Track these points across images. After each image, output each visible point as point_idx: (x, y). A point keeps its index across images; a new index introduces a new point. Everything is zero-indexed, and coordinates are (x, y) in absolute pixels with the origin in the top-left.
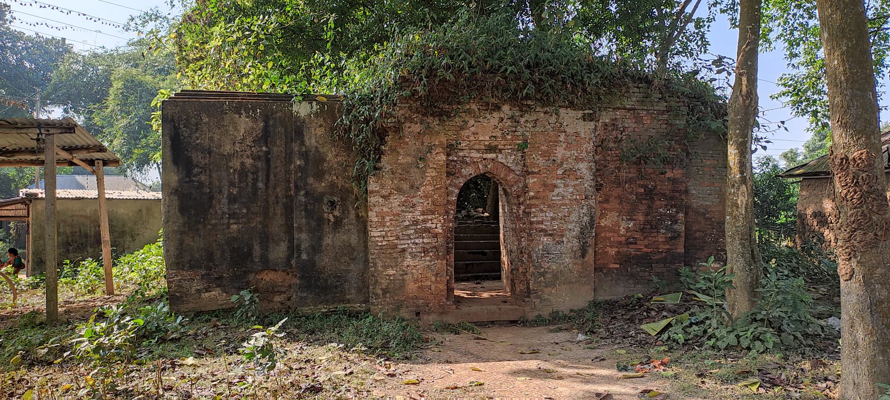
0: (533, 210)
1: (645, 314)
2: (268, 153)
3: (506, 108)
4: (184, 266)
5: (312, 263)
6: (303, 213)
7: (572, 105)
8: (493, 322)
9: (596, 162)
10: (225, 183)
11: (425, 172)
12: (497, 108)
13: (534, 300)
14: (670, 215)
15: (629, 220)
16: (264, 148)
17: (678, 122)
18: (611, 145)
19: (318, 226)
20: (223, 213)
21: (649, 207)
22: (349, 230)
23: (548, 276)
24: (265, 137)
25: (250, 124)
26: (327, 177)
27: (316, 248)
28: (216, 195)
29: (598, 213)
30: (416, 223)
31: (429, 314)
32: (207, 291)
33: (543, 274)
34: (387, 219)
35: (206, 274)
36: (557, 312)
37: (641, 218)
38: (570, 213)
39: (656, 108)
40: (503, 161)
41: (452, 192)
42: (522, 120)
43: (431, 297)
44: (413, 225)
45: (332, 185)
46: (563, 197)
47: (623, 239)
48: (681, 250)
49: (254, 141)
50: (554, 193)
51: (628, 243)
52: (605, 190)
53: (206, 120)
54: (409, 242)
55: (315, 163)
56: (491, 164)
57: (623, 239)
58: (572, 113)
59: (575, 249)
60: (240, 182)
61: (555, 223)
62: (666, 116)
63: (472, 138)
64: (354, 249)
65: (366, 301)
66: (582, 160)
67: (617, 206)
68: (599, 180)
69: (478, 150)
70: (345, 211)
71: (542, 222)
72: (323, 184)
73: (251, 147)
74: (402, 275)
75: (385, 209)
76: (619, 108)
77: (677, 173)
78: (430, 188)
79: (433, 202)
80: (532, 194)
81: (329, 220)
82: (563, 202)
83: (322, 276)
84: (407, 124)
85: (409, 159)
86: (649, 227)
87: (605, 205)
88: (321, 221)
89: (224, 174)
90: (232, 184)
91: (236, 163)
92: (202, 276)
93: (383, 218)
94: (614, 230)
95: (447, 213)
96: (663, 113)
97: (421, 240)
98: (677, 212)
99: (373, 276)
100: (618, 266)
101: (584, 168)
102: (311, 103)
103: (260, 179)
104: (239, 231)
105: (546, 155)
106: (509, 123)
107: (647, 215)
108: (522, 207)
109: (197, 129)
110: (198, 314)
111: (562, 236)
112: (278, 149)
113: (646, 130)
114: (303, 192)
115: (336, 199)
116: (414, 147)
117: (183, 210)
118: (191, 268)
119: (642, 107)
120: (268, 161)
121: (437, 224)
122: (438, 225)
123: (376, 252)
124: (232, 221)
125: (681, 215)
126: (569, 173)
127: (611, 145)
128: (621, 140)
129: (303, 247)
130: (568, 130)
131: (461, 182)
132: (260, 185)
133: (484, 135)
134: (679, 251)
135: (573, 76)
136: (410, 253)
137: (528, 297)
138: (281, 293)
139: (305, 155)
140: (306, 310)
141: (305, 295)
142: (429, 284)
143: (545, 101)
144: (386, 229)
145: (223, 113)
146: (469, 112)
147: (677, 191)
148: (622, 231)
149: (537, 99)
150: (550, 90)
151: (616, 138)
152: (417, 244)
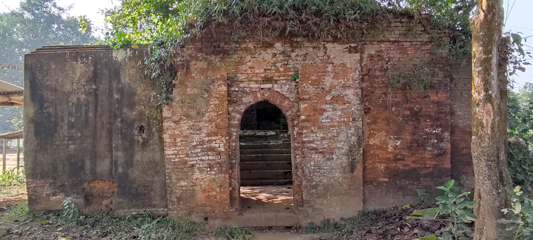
0: (305, 131)
1: (399, 229)
2: (96, 90)
3: (278, 45)
4: (37, 177)
5: (125, 174)
6: (119, 136)
7: (336, 40)
8: (270, 228)
9: (362, 89)
10: (66, 113)
11: (209, 101)
12: (271, 45)
13: (307, 209)
15: (396, 139)
16: (94, 87)
17: (441, 51)
18: (378, 73)
19: (130, 146)
20: (65, 136)
21: (415, 128)
22: (154, 149)
23: (320, 188)
24: (95, 78)
25: (84, 69)
26: (137, 107)
27: (129, 164)
28: (60, 124)
29: (367, 133)
30: (202, 143)
31: (215, 219)
32: (54, 195)
33: (315, 187)
34: (178, 140)
35: (52, 183)
36: (328, 220)
37: (408, 137)
38: (338, 134)
39: (419, 39)
40: (279, 90)
41: (234, 117)
42: (293, 55)
43: (216, 205)
44: (200, 145)
45: (141, 113)
46: (332, 120)
47: (391, 156)
48: (448, 165)
49: (86, 82)
50: (323, 117)
51: (396, 160)
52: (374, 113)
53: (53, 67)
54: (197, 159)
55: (128, 97)
56: (268, 93)
58: (338, 47)
59: (344, 165)
60: (77, 113)
61: (324, 142)
62: (429, 47)
63: (249, 72)
64: (157, 164)
65: (167, 207)
66: (349, 87)
67: (385, 127)
68: (367, 104)
69: (256, 82)
70: (151, 134)
71: (313, 142)
72: (134, 113)
73: (84, 86)
74: (192, 186)
75: (176, 132)
76: (383, 41)
77: (442, 96)
78: (214, 114)
79: (216, 126)
80: (303, 117)
81: (139, 142)
82: (332, 124)
83: (134, 185)
84: (194, 62)
85: (196, 91)
86: (416, 145)
87: (373, 126)
88: (132, 142)
89: (65, 107)
90: (70, 114)
91: (73, 99)
92: (50, 184)
93: (175, 139)
94: (383, 147)
95: (230, 135)
96: (426, 43)
97: (207, 158)
98: (443, 132)
99: (169, 187)
100: (387, 180)
101: (351, 94)
102: (126, 50)
103: (90, 110)
104: (75, 150)
105: (317, 83)
106: (281, 57)
107: (414, 134)
108: (296, 129)
109: (47, 74)
110: (48, 212)
111: (332, 154)
112: (103, 87)
113: (411, 60)
114: (119, 120)
115: (143, 124)
116: (200, 81)
117: (37, 134)
118: (42, 178)
119: (406, 39)
120: (96, 96)
121: (220, 144)
122: (221, 145)
123: (170, 167)
124: (70, 142)
125: (447, 134)
126: (337, 99)
127: (378, 73)
128: (387, 69)
129: (119, 163)
130: (335, 62)
132: (91, 115)
134: (445, 166)
135: (336, 15)
136: (198, 168)
137: (302, 206)
138: (107, 198)
139: (121, 91)
140: (121, 213)
141: (121, 200)
142: (214, 193)
143: (311, 37)
144: (177, 148)
145: (65, 61)
146: (246, 50)
147: (441, 113)
148: (390, 149)
149: (304, 36)
150: (315, 29)
151: (382, 67)
152: (203, 160)
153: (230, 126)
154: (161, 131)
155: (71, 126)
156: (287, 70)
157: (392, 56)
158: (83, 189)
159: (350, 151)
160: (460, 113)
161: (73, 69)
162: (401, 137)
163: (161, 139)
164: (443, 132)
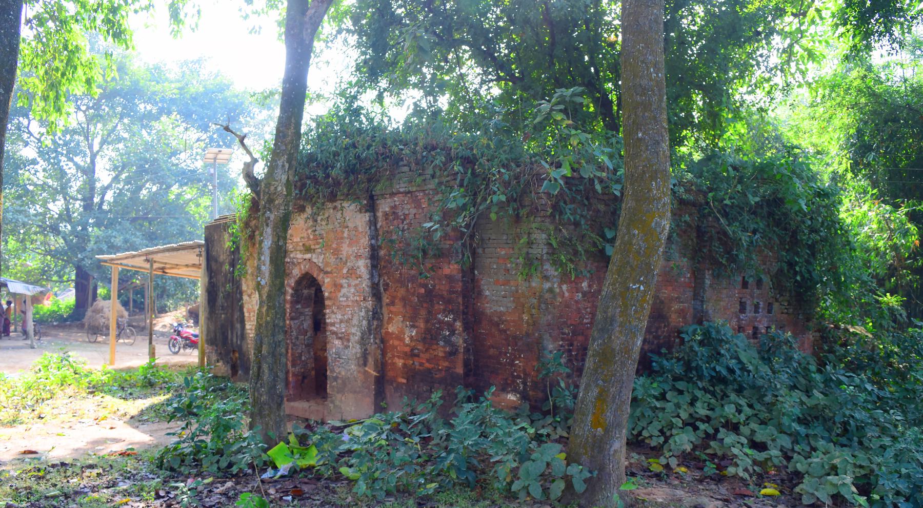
14: (448, 323)
21: (429, 312)
23: (340, 381)
37: (422, 325)
40: (315, 260)
46: (347, 298)
47: (407, 349)
57: (407, 349)
61: (343, 325)
67: (402, 310)
86: (429, 337)
87: (392, 308)
98: (455, 320)
148: (407, 341)
157: (407, 212)
158: (231, 359)
159: (362, 338)
160: (487, 293)
162: (417, 324)
164: (455, 320)
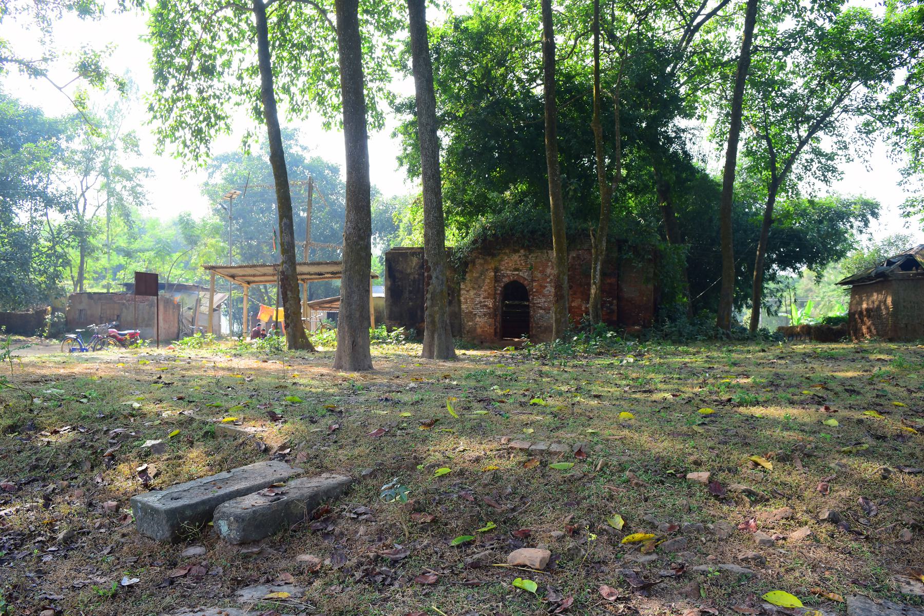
3: (522, 251)
12: (518, 251)
30: (481, 302)
33: (540, 327)
48: (615, 318)
91: (412, 277)
95: (495, 298)
105: (543, 272)
121: (490, 303)
125: (615, 302)
131: (502, 284)
133: (513, 265)
146: (505, 253)
153: (495, 294)
154: (459, 295)
155: (410, 292)
156: (526, 264)
161: (412, 261)
163: (459, 301)
